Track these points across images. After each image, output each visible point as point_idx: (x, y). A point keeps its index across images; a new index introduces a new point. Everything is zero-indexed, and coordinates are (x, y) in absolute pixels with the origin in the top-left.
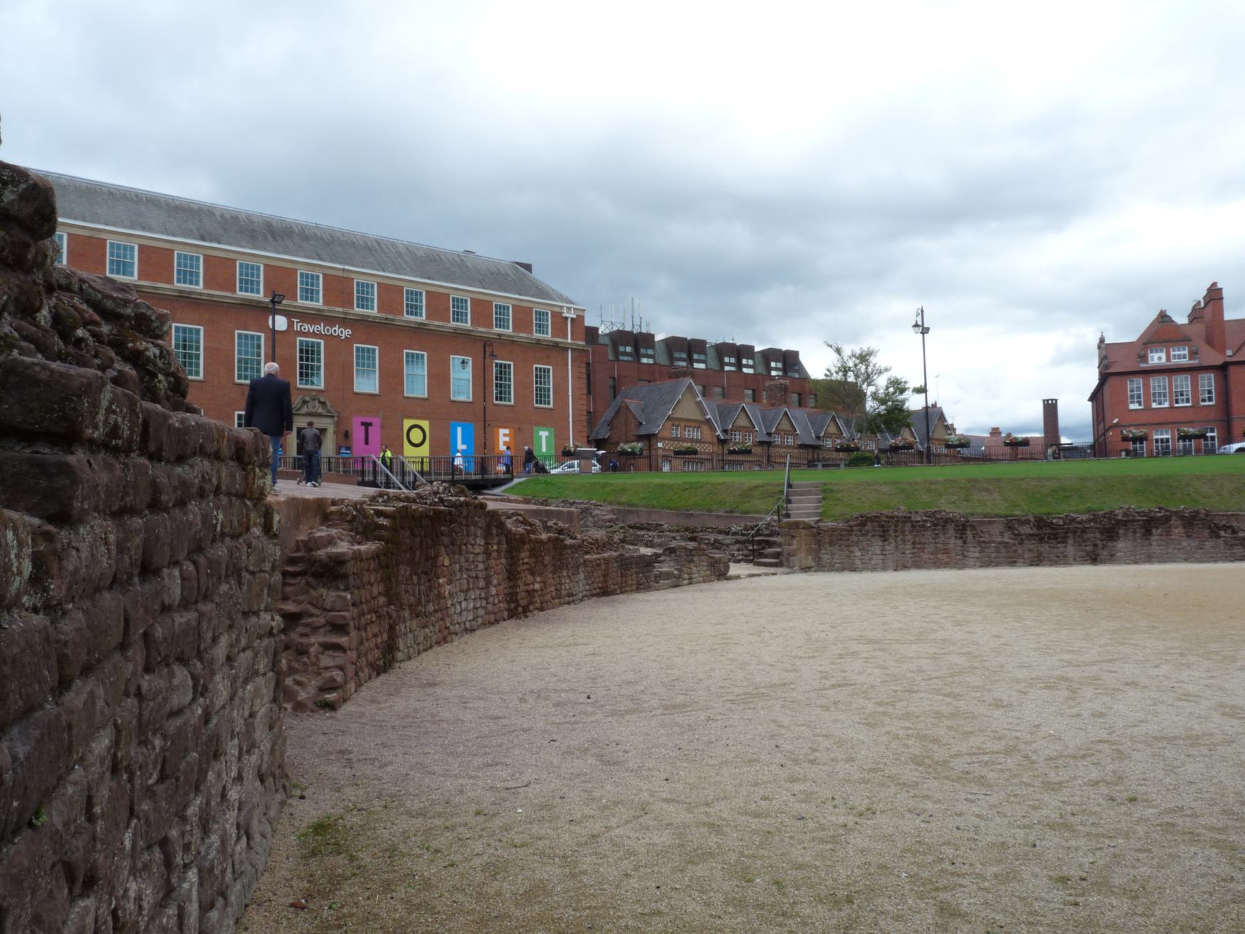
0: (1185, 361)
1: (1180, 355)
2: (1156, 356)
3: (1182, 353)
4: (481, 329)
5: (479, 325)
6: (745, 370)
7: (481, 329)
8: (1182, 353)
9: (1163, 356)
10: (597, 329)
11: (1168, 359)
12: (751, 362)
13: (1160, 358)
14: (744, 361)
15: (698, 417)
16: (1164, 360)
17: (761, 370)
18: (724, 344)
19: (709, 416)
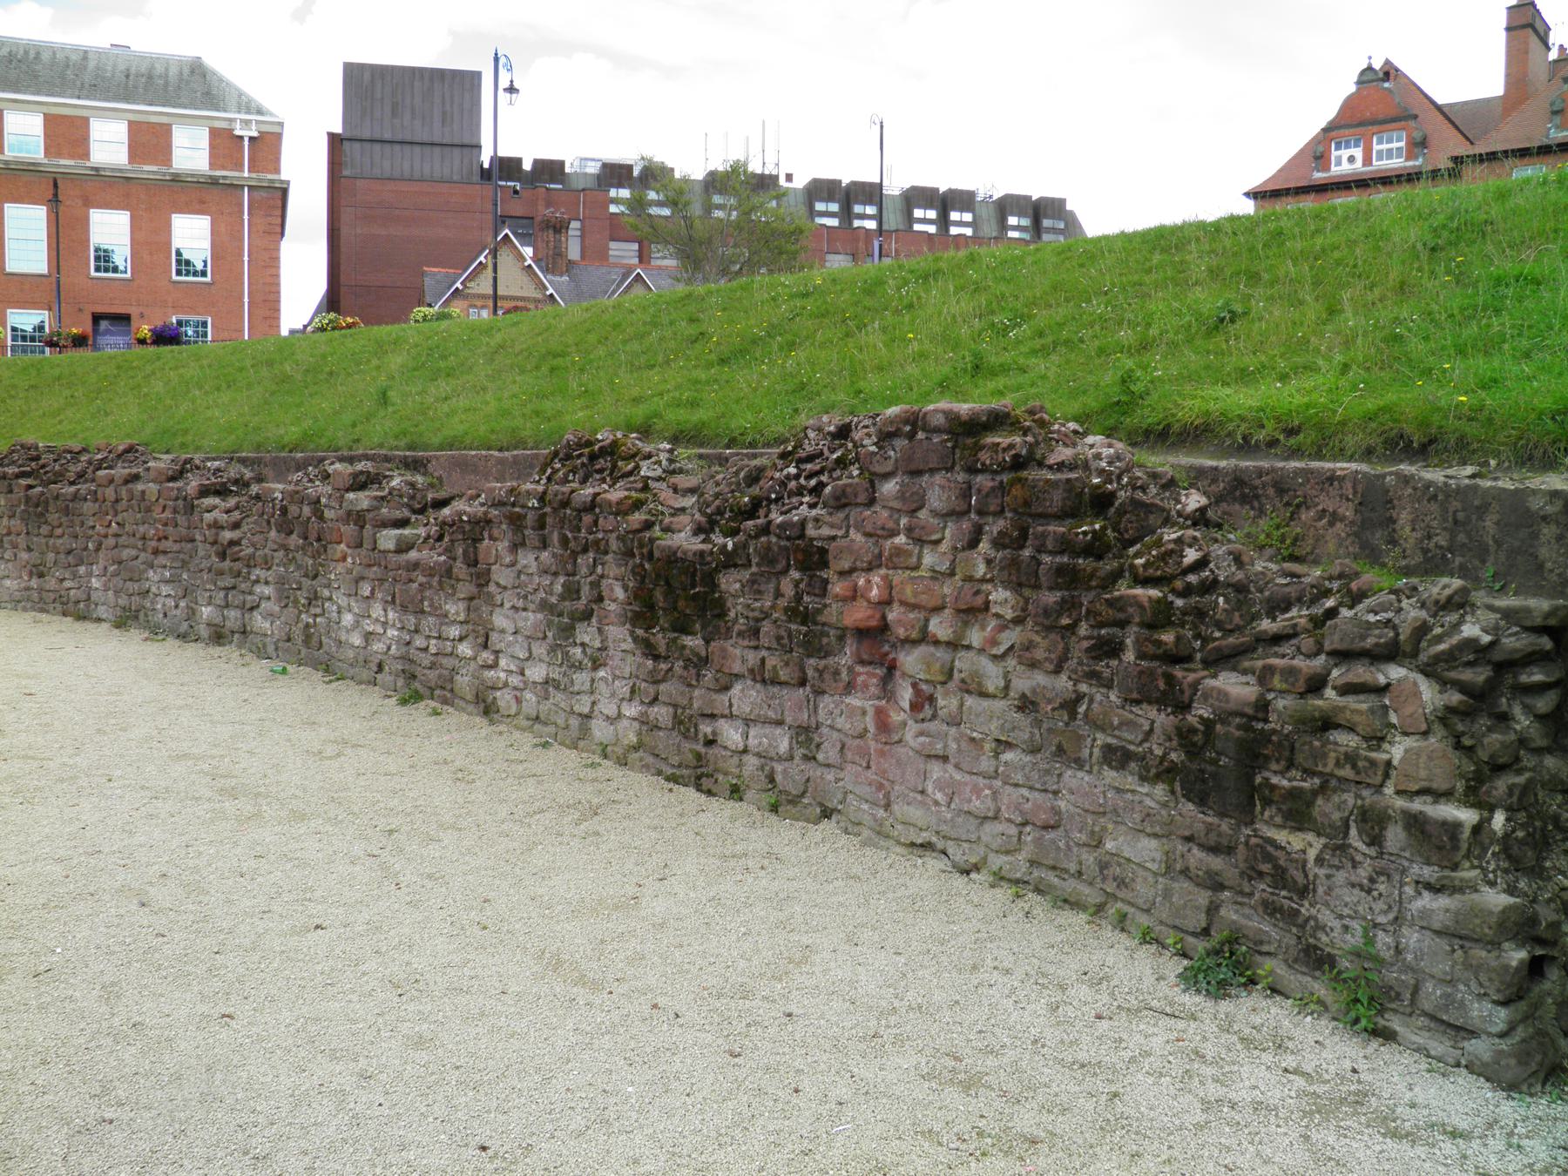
0: (1397, 163)
1: (1390, 153)
2: (1345, 154)
3: (1395, 145)
4: (63, 162)
5: (60, 155)
6: (654, 211)
7: (63, 162)
8: (1395, 145)
9: (1358, 153)
10: (562, 163)
11: (1367, 160)
12: (968, 217)
13: (1351, 159)
14: (954, 216)
15: (530, 292)
16: (1359, 164)
17: (989, 230)
18: (914, 189)
19: (551, 291)
